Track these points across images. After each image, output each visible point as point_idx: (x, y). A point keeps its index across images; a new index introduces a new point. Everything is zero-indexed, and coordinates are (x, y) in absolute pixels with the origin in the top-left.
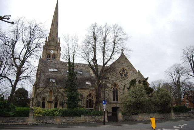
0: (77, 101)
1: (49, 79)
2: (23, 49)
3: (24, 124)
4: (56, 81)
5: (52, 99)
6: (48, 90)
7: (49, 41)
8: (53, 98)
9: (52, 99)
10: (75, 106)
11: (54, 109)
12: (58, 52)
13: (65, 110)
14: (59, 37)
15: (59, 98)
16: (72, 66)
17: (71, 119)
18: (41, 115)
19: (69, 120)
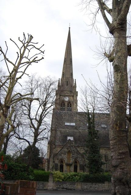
0: (100, 164)
1: (66, 137)
2: (39, 109)
3: (45, 189)
4: (74, 139)
5: (71, 161)
6: (66, 150)
7: (63, 85)
8: (72, 161)
9: (71, 161)
10: (98, 170)
11: (73, 173)
12: (75, 98)
13: (87, 175)
14: (74, 78)
15: (79, 160)
16: (92, 123)
17: (93, 185)
18: (61, 180)
19: (91, 187)
